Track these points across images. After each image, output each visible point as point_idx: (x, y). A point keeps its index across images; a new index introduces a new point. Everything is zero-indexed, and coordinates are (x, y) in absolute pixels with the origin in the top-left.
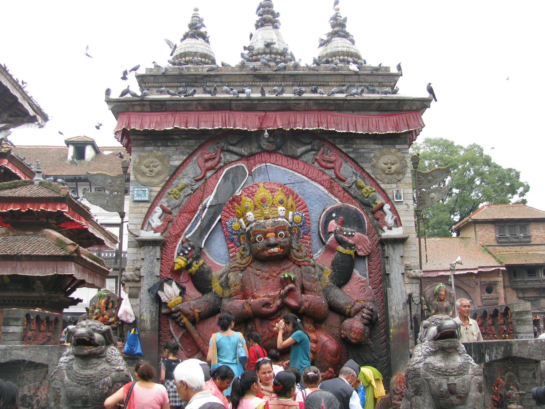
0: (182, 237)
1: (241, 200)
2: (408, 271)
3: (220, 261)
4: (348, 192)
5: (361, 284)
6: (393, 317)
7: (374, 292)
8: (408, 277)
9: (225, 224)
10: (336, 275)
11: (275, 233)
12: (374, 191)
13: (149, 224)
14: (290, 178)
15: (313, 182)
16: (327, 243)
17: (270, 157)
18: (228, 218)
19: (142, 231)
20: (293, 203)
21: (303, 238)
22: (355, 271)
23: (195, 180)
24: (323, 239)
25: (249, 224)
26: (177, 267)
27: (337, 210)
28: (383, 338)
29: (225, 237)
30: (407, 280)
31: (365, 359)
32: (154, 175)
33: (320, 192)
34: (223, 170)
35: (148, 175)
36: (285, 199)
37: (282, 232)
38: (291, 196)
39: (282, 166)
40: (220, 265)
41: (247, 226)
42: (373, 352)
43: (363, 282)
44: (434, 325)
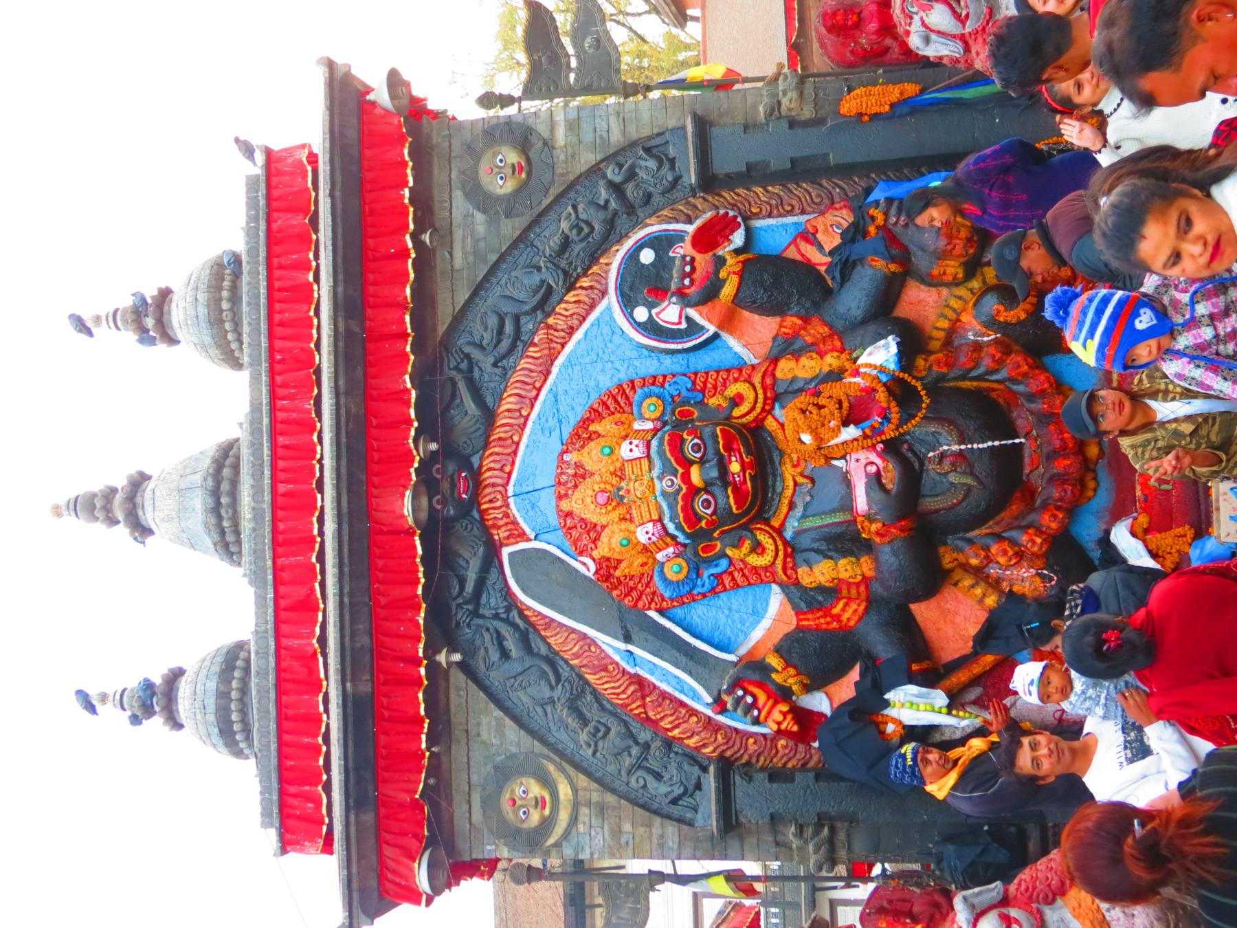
0: (709, 712)
1: (608, 559)
4: (578, 278)
9: (672, 600)
12: (575, 207)
13: (674, 802)
15: (555, 370)
17: (493, 485)
18: (654, 593)
19: (699, 822)
21: (703, 391)
23: (557, 683)
26: (789, 725)
27: (628, 303)
29: (704, 596)
32: (548, 798)
34: (529, 608)
35: (547, 812)
39: (515, 453)
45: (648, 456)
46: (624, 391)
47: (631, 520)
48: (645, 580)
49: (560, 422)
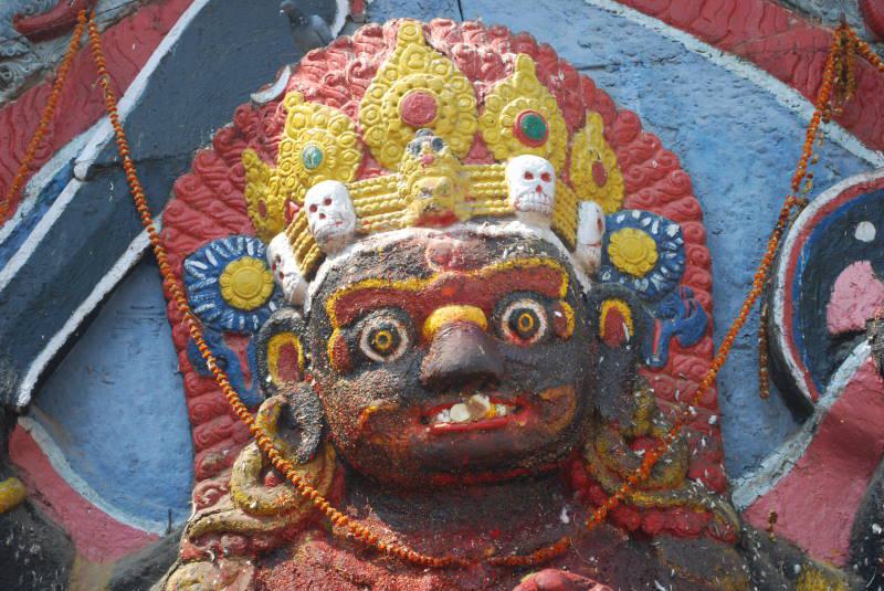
3: (133, 498)
11: (488, 311)
14: (592, 38)
16: (826, 402)
20: (610, 160)
23: (20, 29)
24: (799, 375)
25: (320, 260)
29: (179, 349)
33: (771, 112)
36: (556, 124)
37: (535, 307)
38: (594, 123)
40: (135, 524)
41: (310, 276)
45: (509, 216)
46: (675, 197)
47: (361, 173)
48: (230, 215)
49: (616, 66)
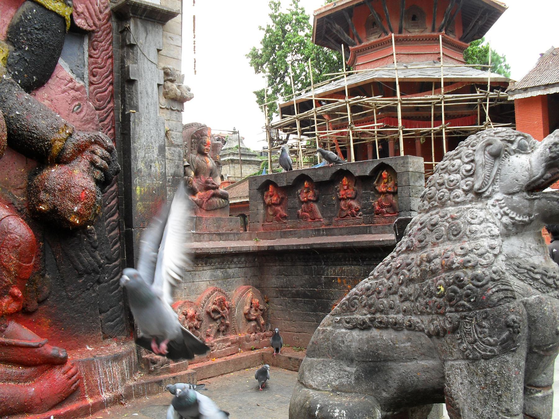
2: (169, 84)
5: (73, 93)
6: (140, 171)
7: (99, 116)
8: (166, 95)
10: (21, 58)
22: (61, 62)
28: (115, 217)
30: (163, 101)
31: (81, 266)
42: (96, 248)
43: (77, 90)
44: (515, 152)
